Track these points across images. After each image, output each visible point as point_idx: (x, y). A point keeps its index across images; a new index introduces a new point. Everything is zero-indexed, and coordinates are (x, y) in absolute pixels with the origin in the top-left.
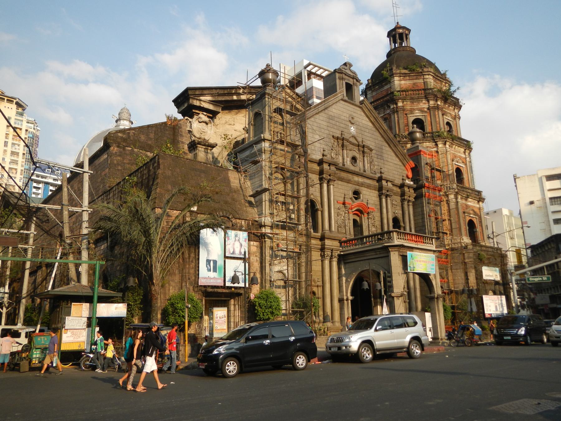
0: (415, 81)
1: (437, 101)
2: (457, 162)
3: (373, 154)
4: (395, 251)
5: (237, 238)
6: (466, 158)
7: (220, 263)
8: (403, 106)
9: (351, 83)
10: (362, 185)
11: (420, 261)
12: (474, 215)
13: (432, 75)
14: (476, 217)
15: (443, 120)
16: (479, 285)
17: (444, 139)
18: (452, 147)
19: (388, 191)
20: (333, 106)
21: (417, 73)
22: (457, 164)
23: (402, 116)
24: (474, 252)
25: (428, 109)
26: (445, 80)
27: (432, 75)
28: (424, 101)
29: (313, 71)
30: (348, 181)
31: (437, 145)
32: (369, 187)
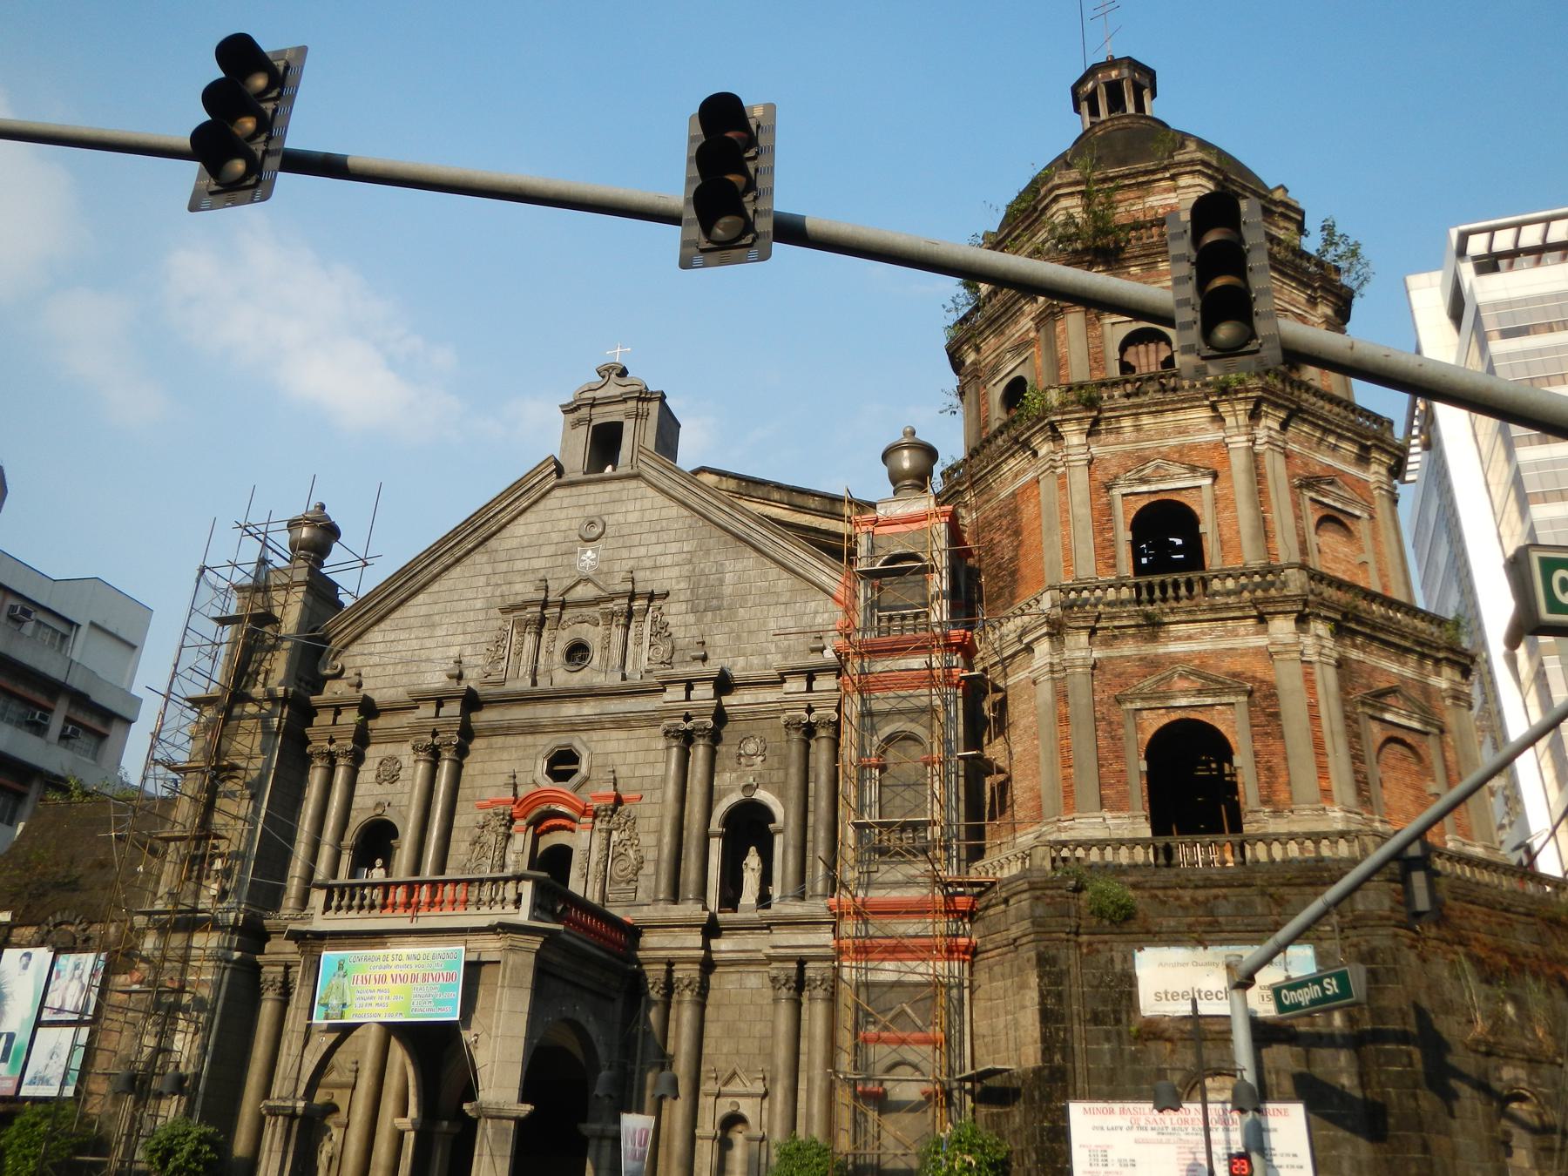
2: (1143, 481)
3: (664, 610)
5: (78, 973)
6: (1223, 445)
7: (22, 1039)
8: (973, 363)
10: (591, 725)
11: (383, 979)
12: (1200, 692)
13: (1072, 194)
14: (1225, 700)
15: (1102, 336)
16: (1068, 1052)
17: (1040, 419)
18: (1118, 430)
19: (687, 718)
20: (521, 520)
21: (1028, 217)
22: (1144, 488)
23: (973, 398)
24: (1033, 887)
25: (1038, 331)
26: (1166, 168)
27: (1072, 194)
29: (1504, 241)
30: (533, 729)
31: (1035, 454)
32: (622, 723)
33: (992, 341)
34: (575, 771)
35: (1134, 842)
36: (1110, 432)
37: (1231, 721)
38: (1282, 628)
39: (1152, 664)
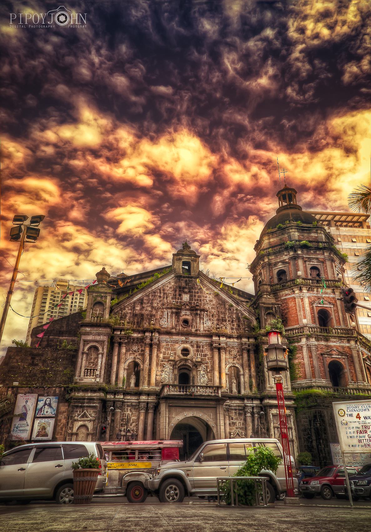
0: (280, 237)
1: (295, 251)
2: (320, 304)
4: (164, 403)
8: (268, 262)
9: (190, 261)
12: (338, 355)
14: (344, 357)
15: (306, 266)
18: (313, 291)
22: (320, 305)
27: (295, 228)
28: (286, 254)
31: (294, 292)
33: (273, 257)
34: (189, 354)
35: (327, 387)
36: (312, 290)
37: (344, 362)
38: (353, 343)
39: (328, 347)
